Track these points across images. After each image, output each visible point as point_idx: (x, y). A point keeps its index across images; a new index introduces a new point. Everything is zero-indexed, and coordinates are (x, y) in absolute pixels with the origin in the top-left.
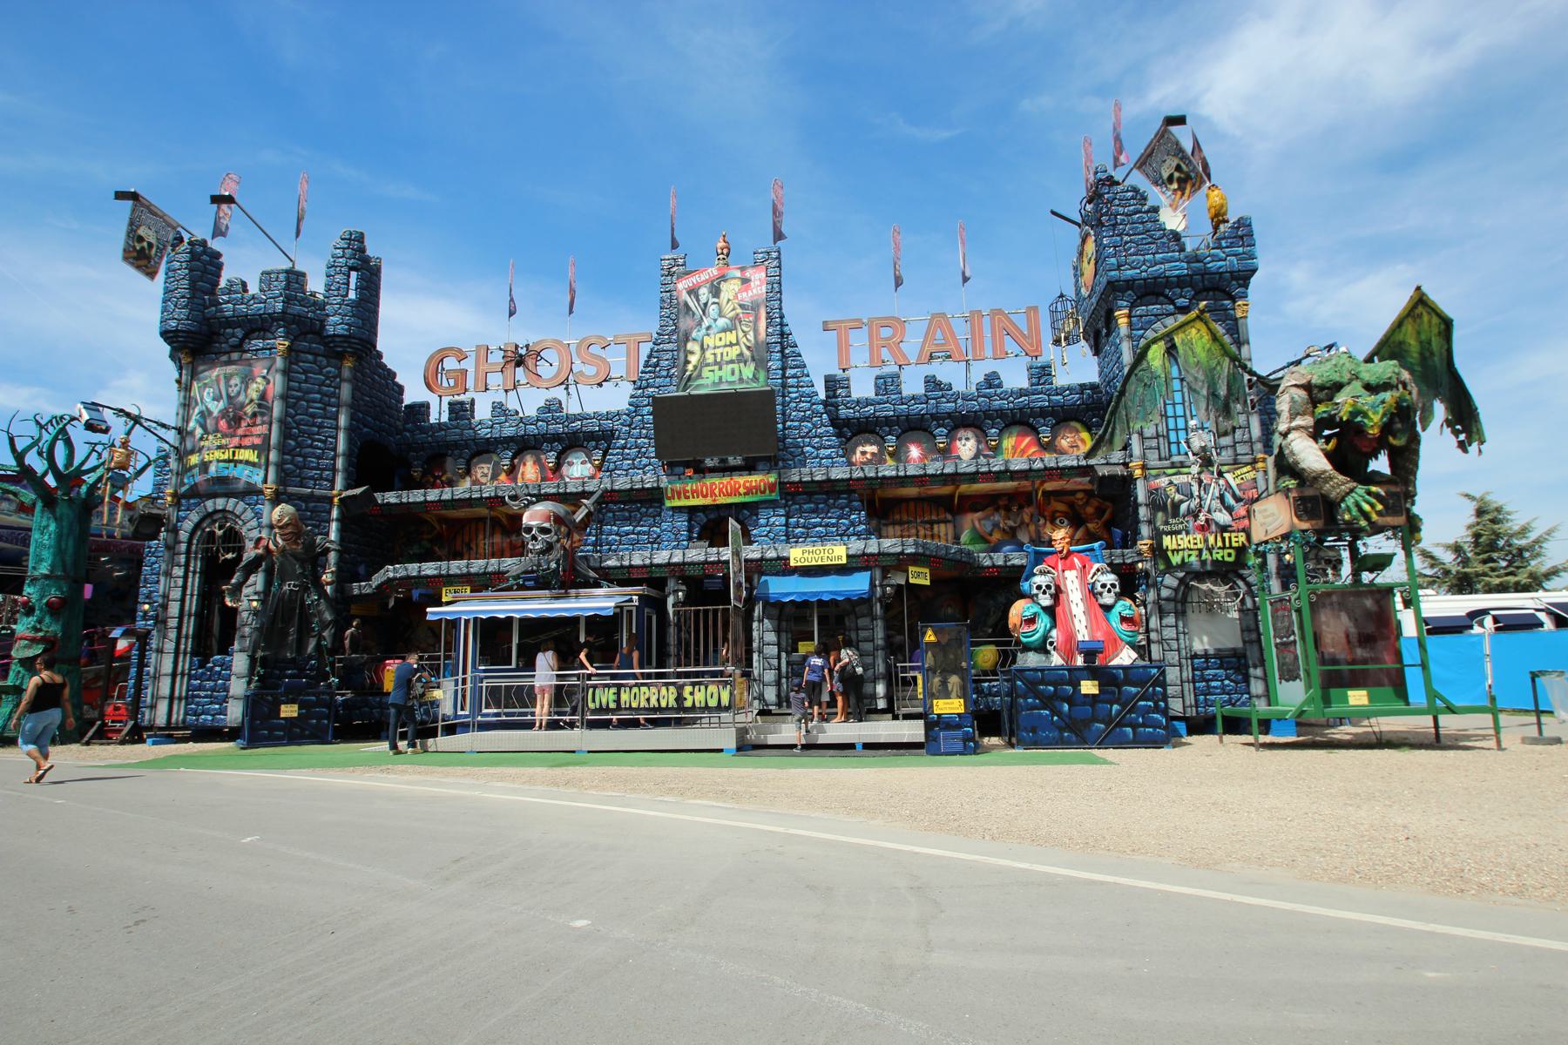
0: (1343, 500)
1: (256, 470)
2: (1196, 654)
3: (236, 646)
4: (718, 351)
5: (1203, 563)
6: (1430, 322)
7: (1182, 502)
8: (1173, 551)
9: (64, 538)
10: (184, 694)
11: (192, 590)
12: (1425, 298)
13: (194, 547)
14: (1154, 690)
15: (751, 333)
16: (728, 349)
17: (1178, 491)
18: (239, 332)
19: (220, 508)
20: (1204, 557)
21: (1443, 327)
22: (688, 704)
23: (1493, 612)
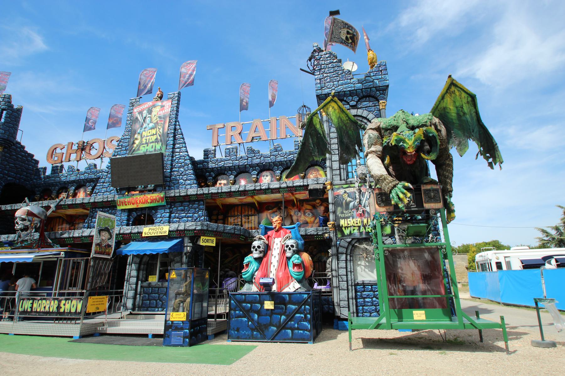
0: (391, 192)
2: (358, 283)
4: (148, 138)
5: (361, 233)
6: (460, 95)
7: (351, 202)
8: (345, 227)
12: (454, 82)
14: (305, 307)
15: (162, 129)
16: (152, 137)
17: (349, 196)
20: (361, 231)
21: (470, 99)
22: (62, 310)
23: (555, 257)
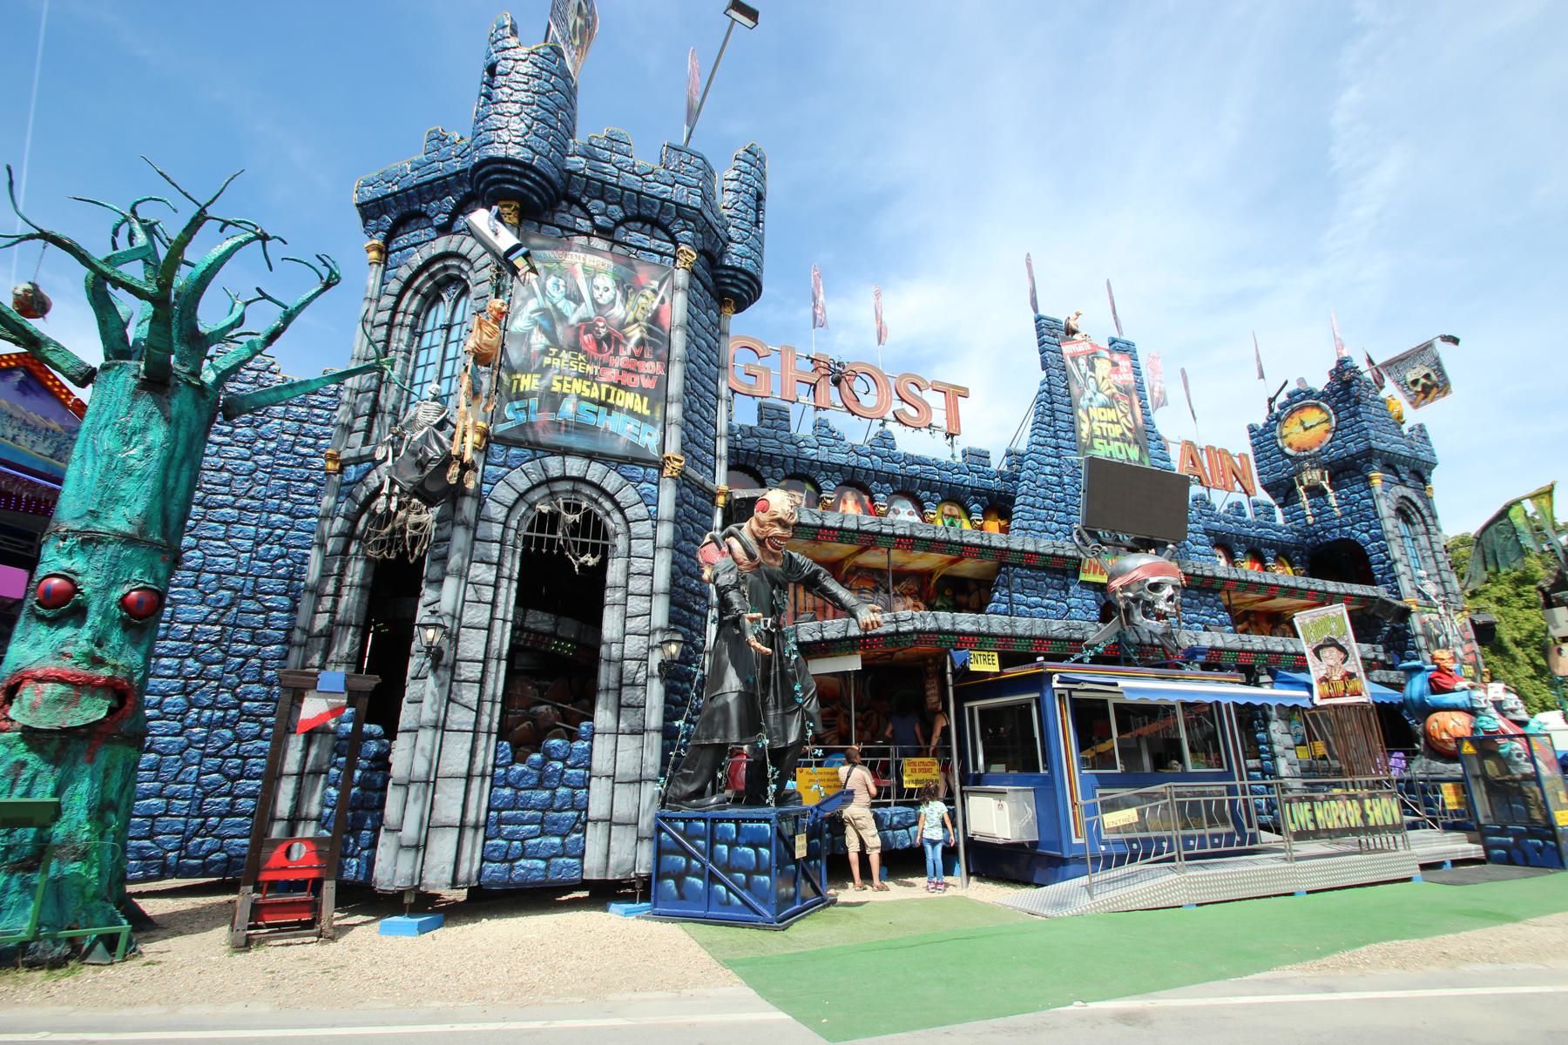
1: (646, 427)
3: (603, 717)
9: (176, 462)
10: (483, 817)
13: (512, 533)
16: (1110, 426)
18: (617, 212)
19: (574, 474)
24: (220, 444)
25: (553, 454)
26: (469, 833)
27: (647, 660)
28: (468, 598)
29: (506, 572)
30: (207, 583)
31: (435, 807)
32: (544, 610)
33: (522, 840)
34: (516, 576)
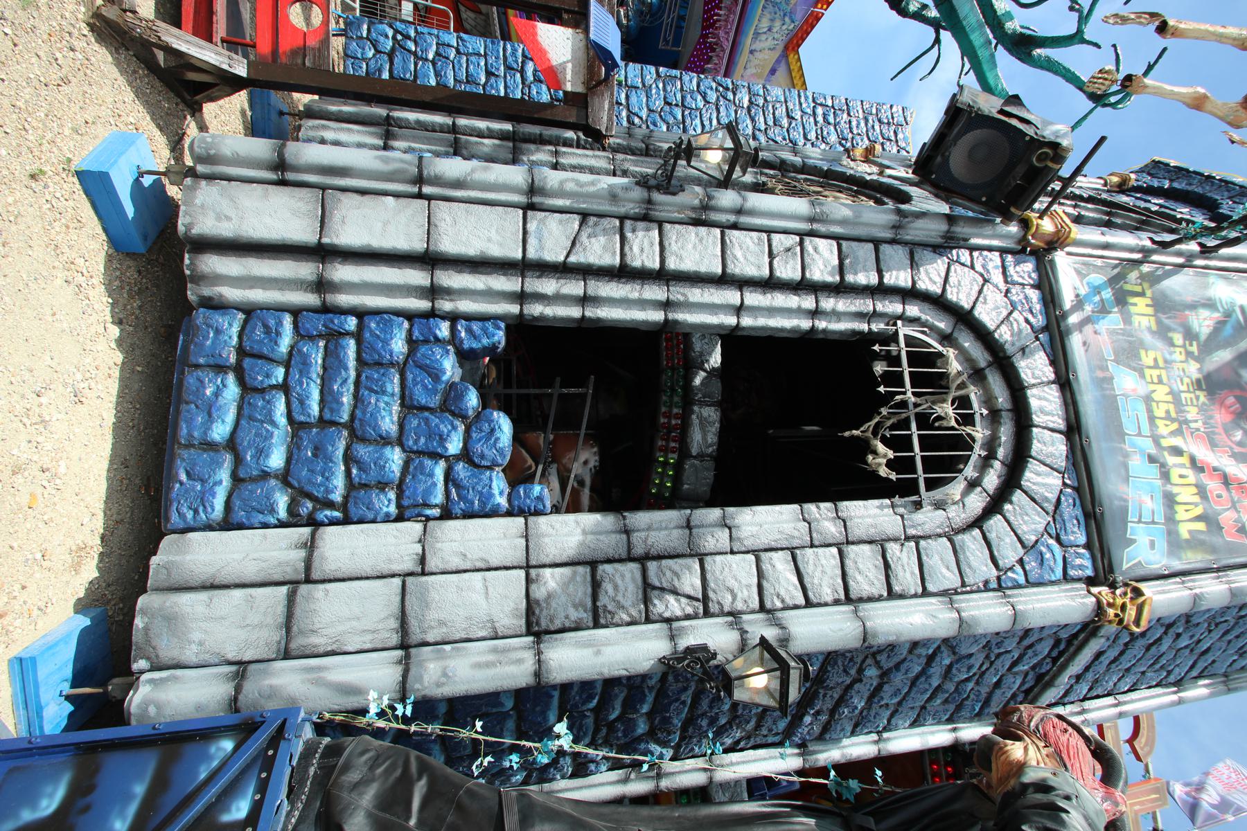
10: (344, 299)
11: (756, 310)
13: (895, 307)
24: (814, 114)
25: (1053, 363)
26: (306, 270)
27: (707, 614)
28: (776, 238)
29: (828, 303)
30: (671, 113)
31: (367, 198)
32: (722, 433)
33: (285, 387)
34: (821, 324)
